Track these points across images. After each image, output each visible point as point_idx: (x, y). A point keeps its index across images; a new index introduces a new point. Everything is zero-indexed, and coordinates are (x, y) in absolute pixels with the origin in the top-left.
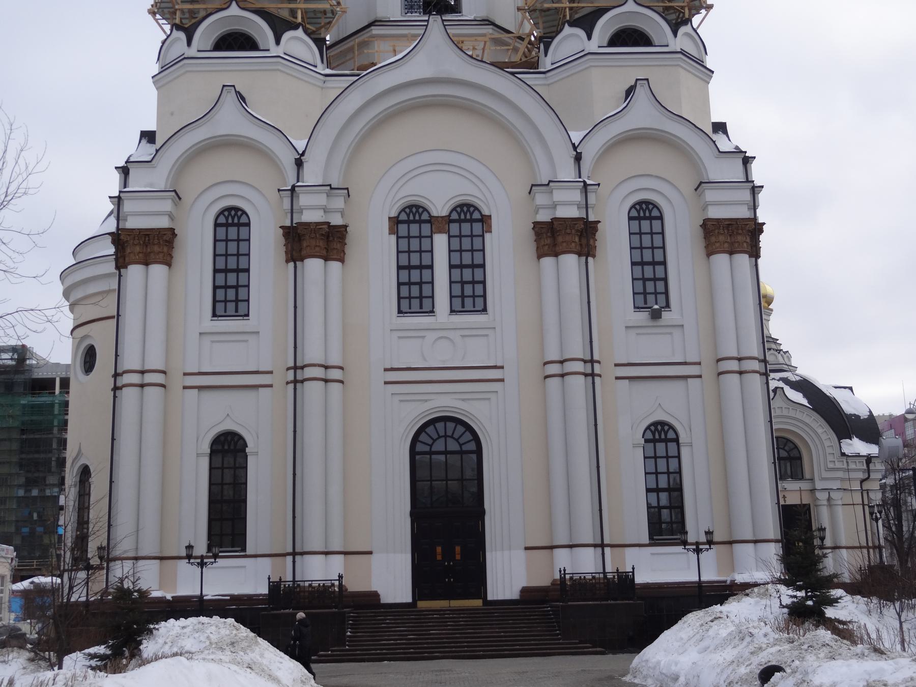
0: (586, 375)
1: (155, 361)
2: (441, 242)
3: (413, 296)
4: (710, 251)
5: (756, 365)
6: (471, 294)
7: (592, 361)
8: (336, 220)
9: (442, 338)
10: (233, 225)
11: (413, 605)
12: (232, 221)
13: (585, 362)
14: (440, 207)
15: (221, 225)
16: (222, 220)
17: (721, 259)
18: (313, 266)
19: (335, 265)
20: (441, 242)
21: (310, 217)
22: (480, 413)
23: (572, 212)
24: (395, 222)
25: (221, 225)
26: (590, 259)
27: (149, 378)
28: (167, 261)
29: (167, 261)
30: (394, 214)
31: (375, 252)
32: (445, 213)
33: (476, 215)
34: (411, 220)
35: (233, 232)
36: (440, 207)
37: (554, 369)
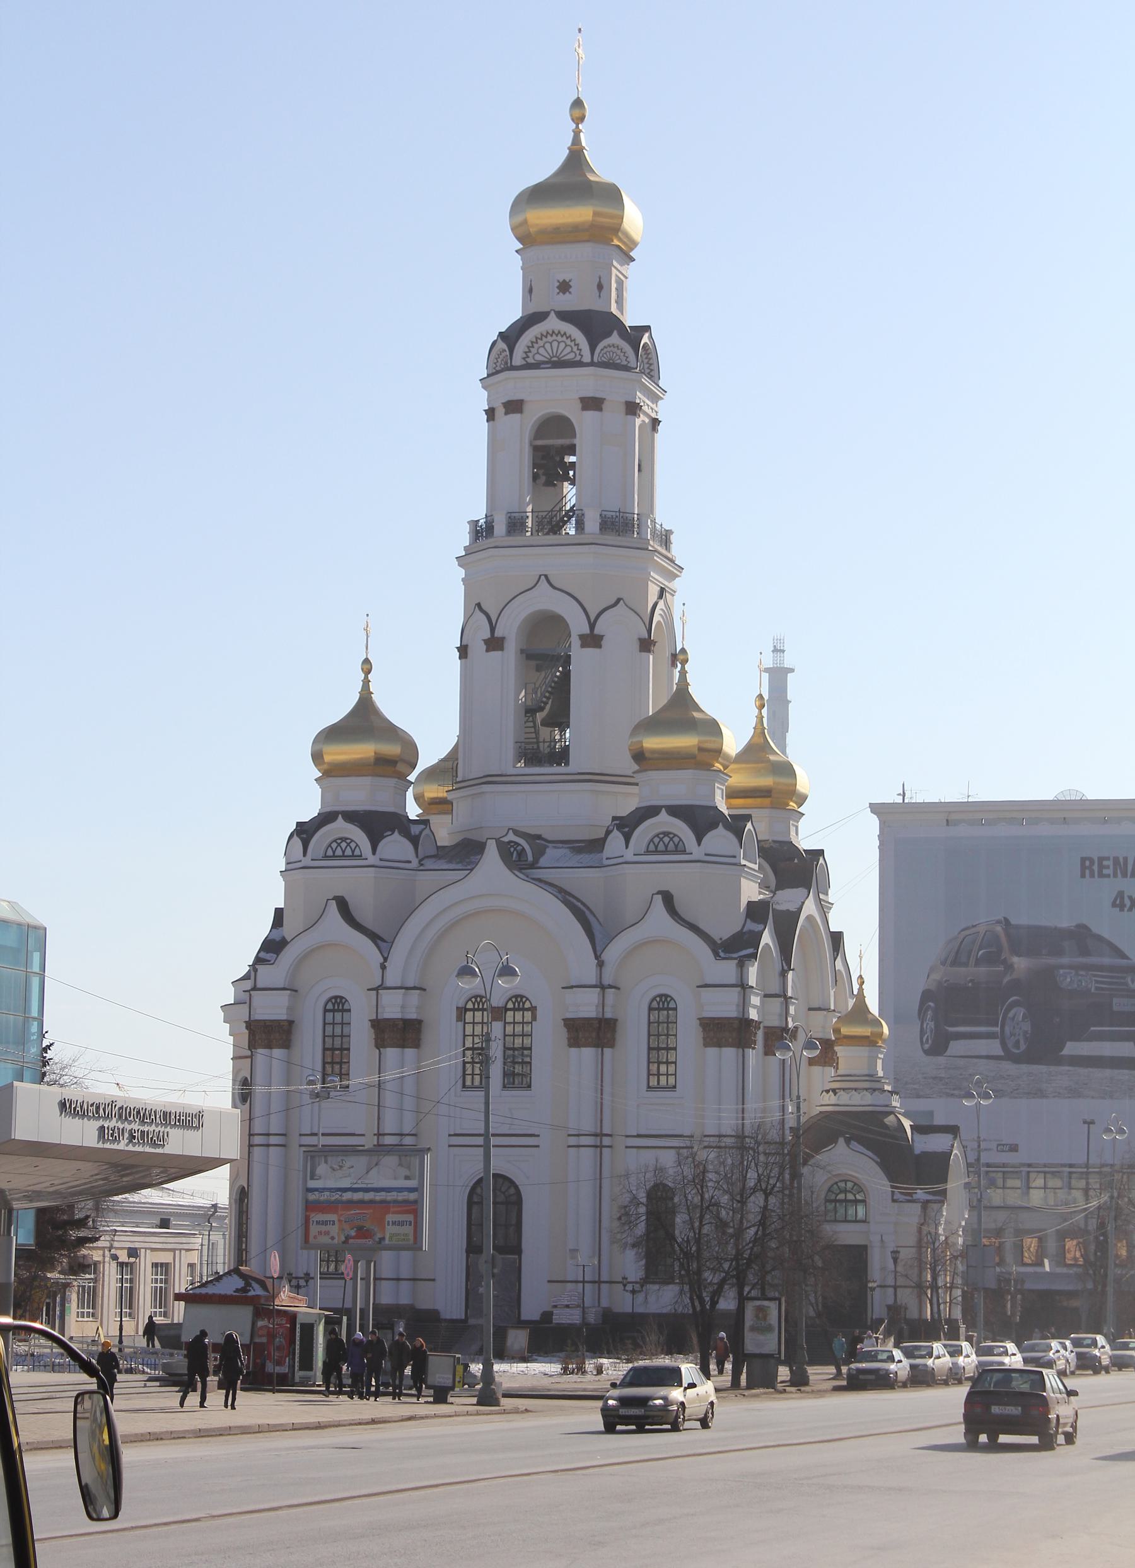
0: (596, 1146)
1: (399, 1009)
4: (707, 1044)
6: (518, 1074)
7: (600, 1135)
8: (412, 1015)
10: (338, 1010)
11: (465, 1321)
13: (596, 1135)
15: (329, 1011)
16: (330, 1006)
17: (712, 1052)
19: (410, 1052)
25: (329, 1011)
26: (607, 1051)
27: (273, 1140)
28: (286, 1044)
29: (286, 1044)
30: (461, 1004)
32: (501, 1004)
33: (527, 1005)
35: (338, 1016)
37: (573, 1141)
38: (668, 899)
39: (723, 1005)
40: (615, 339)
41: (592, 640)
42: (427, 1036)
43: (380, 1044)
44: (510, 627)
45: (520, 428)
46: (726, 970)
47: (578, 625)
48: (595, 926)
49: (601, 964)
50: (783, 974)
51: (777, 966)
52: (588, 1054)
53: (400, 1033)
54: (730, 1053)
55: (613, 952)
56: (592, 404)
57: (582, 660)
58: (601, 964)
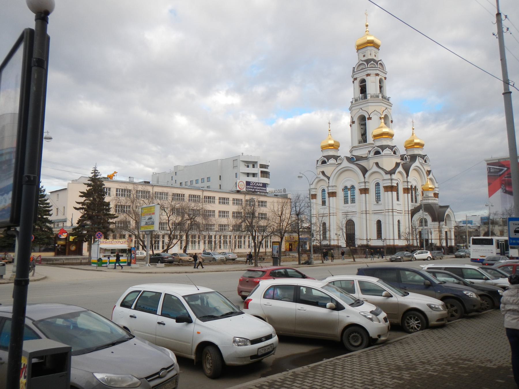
2: (349, 192)
3: (346, 202)
5: (391, 211)
6: (353, 201)
9: (350, 207)
12: (323, 190)
14: (349, 187)
18: (331, 198)
20: (349, 192)
21: (330, 191)
22: (355, 220)
23: (363, 187)
24: (343, 190)
29: (316, 198)
31: (341, 194)
34: (345, 189)
36: (349, 187)
38: (377, 164)
39: (388, 184)
40: (372, 62)
41: (370, 118)
42: (337, 195)
43: (329, 197)
44: (356, 119)
45: (357, 82)
46: (388, 176)
47: (367, 116)
48: (364, 171)
49: (365, 178)
50: (407, 177)
51: (405, 175)
52: (364, 195)
53: (333, 194)
54: (390, 193)
55: (367, 175)
56: (368, 75)
57: (368, 122)
58: (365, 178)
